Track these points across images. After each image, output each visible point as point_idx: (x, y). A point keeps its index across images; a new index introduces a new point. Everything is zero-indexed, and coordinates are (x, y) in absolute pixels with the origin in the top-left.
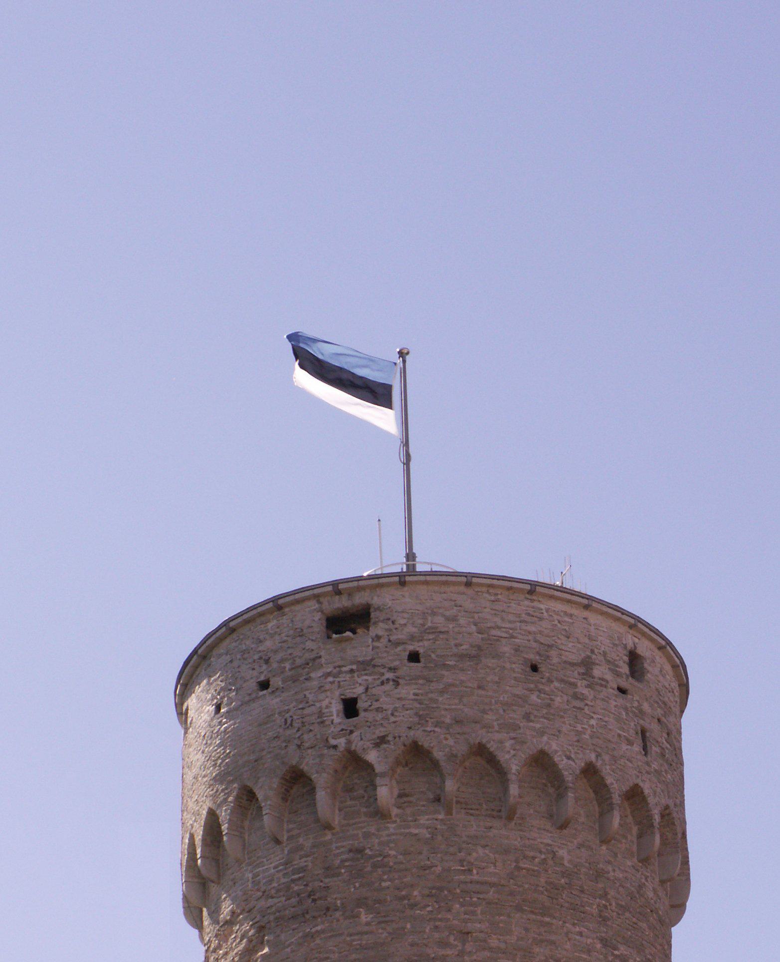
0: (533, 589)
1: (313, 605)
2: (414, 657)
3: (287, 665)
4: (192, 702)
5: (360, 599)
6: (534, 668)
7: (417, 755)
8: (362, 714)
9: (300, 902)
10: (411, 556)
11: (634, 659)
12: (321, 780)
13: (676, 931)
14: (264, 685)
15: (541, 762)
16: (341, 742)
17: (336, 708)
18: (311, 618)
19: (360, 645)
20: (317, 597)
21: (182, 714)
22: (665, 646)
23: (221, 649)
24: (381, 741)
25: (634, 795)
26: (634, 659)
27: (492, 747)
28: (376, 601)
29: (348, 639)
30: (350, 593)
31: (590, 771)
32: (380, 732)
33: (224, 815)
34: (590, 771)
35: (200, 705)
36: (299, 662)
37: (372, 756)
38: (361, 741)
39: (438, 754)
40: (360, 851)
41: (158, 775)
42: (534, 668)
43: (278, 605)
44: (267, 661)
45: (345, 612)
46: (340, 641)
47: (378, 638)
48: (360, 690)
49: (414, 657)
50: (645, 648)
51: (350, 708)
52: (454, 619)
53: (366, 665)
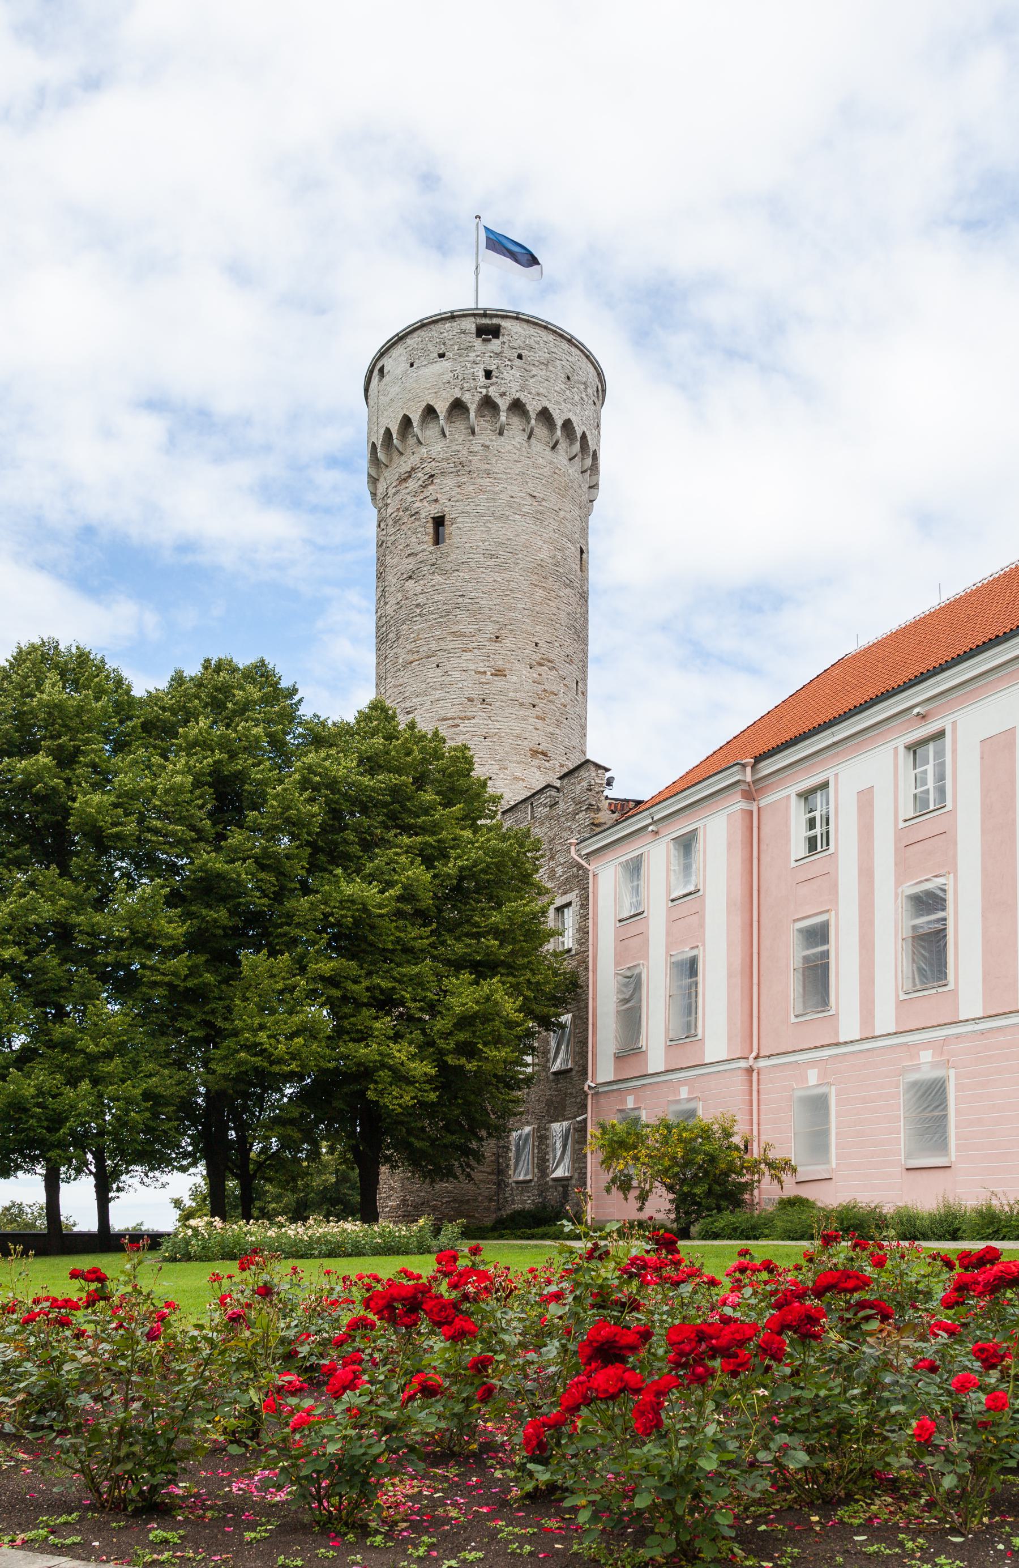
1: (472, 319)
2: (520, 357)
3: (456, 347)
5: (495, 321)
6: (568, 378)
7: (517, 407)
8: (494, 379)
9: (455, 467)
12: (473, 408)
14: (442, 356)
16: (484, 391)
17: (481, 373)
18: (470, 325)
19: (495, 344)
20: (474, 315)
23: (415, 335)
24: (503, 395)
27: (551, 410)
28: (504, 323)
29: (489, 340)
30: (492, 316)
32: (503, 390)
36: (462, 347)
37: (499, 401)
38: (493, 392)
39: (529, 408)
40: (488, 447)
42: (568, 378)
44: (444, 344)
46: (484, 340)
47: (504, 343)
48: (493, 367)
49: (520, 357)
51: (488, 374)
52: (538, 343)
53: (497, 355)
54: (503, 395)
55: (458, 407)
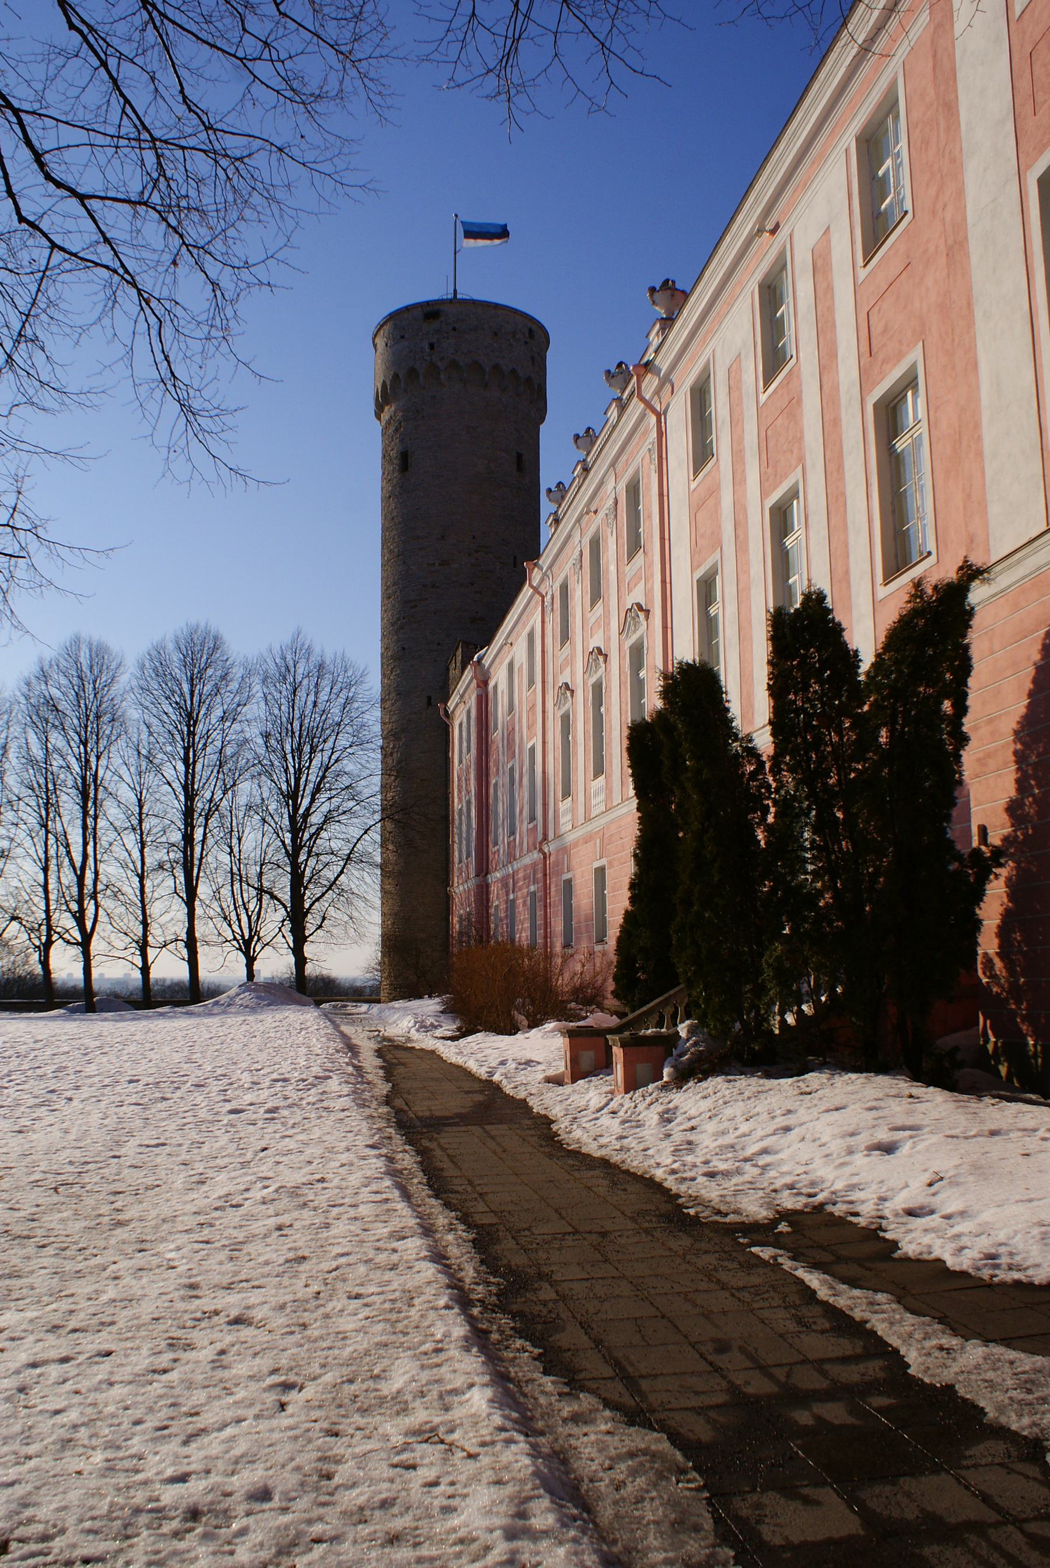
0: (496, 306)
2: (454, 329)
4: (377, 340)
7: (454, 364)
10: (455, 291)
11: (531, 331)
13: (543, 427)
14: (403, 337)
15: (496, 367)
17: (427, 347)
21: (375, 346)
22: (542, 327)
24: (442, 359)
25: (529, 380)
26: (531, 331)
31: (513, 371)
33: (388, 383)
34: (513, 371)
35: (380, 342)
37: (439, 364)
41: (366, 368)
43: (408, 309)
45: (430, 312)
49: (454, 329)
50: (534, 328)
51: (432, 346)
54: (442, 359)
55: (412, 372)
